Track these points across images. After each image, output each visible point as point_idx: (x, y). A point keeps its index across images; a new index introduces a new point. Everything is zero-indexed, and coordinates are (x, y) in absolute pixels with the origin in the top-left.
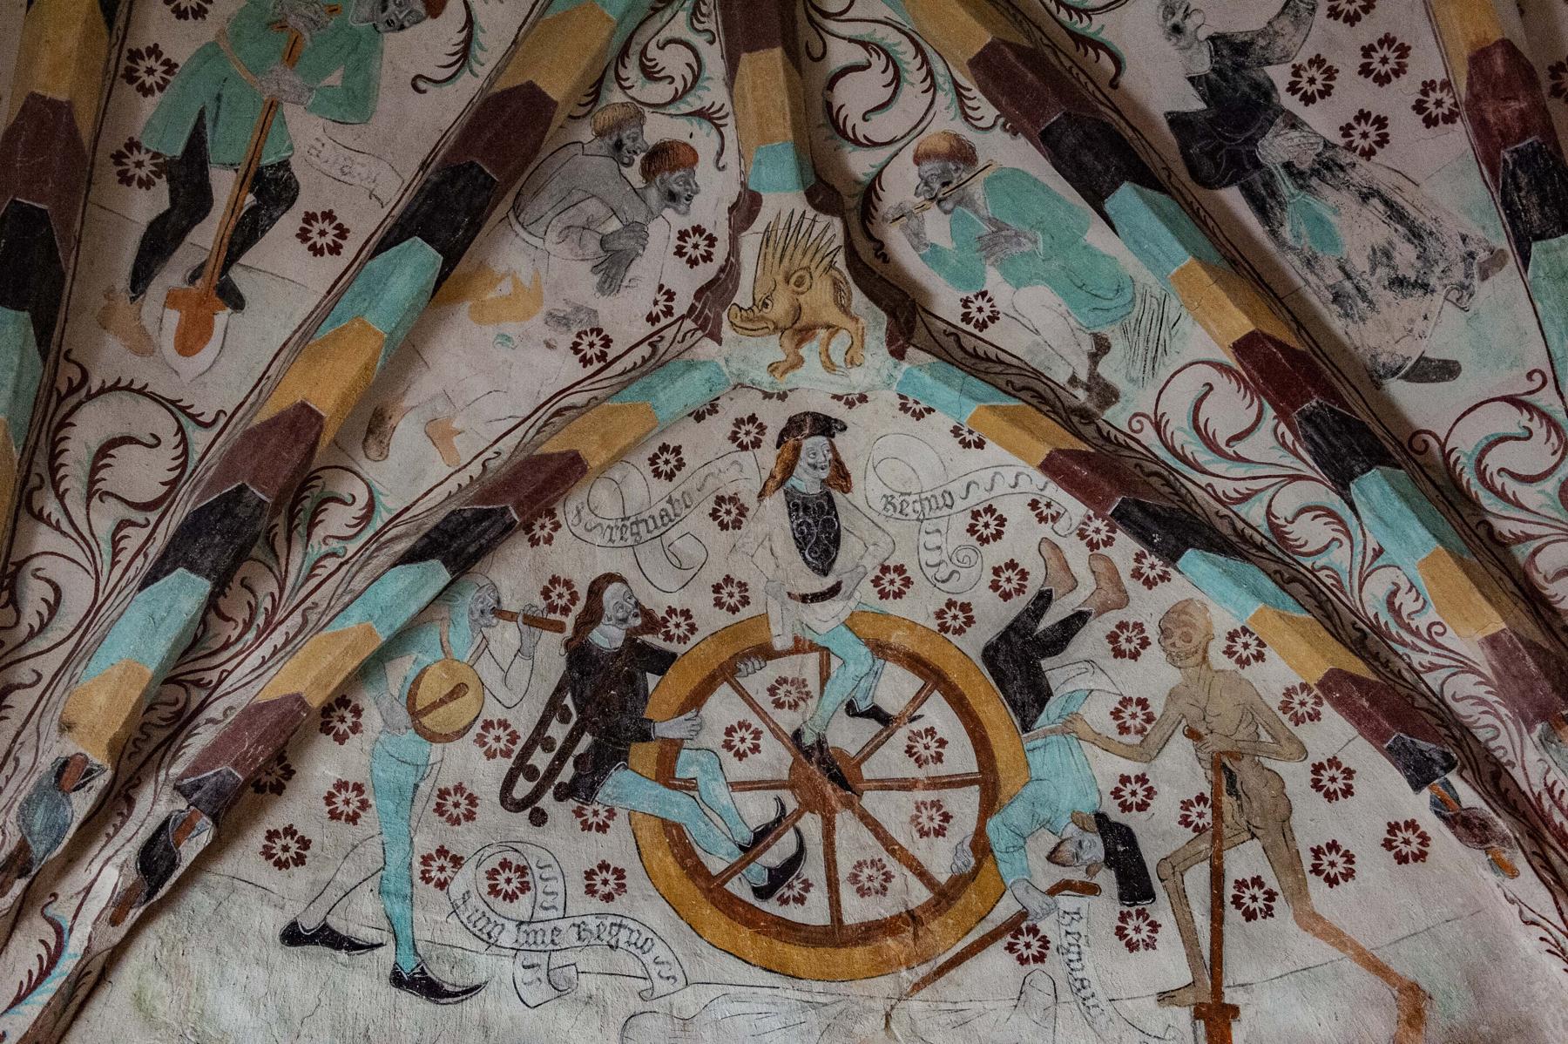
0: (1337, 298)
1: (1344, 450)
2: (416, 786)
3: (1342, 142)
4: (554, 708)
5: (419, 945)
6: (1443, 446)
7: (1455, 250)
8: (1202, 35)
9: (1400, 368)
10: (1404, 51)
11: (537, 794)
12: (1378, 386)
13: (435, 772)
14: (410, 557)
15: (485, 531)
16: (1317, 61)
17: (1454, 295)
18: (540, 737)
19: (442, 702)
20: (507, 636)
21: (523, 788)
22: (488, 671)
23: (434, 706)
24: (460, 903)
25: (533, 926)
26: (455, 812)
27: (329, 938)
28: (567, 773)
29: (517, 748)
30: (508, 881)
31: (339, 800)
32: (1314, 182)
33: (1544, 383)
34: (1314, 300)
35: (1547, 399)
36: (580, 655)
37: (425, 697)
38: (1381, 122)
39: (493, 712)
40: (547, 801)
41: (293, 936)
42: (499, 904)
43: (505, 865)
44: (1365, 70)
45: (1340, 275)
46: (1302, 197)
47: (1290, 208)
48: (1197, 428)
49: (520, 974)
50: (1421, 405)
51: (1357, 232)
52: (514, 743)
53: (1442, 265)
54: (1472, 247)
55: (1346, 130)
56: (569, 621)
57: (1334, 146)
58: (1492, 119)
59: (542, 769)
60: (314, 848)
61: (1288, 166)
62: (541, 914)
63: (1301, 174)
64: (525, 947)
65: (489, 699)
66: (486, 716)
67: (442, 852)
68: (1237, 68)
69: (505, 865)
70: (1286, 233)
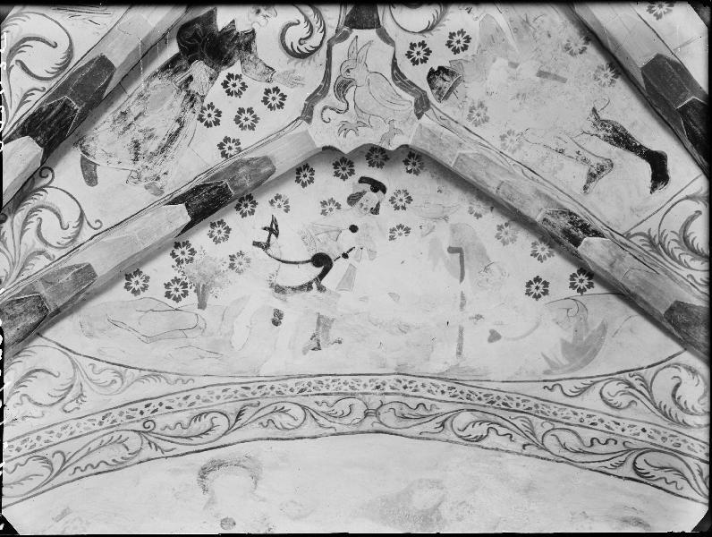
0: (124, 114)
1: (49, 129)
3: (205, 105)
6: (46, 186)
7: (157, 170)
8: (256, 27)
9: (87, 154)
10: (252, 127)
12: (75, 144)
16: (244, 87)
17: (134, 174)
32: (184, 93)
33: (95, 229)
34: (120, 102)
35: (87, 232)
38: (217, 123)
44: (241, 111)
45: (136, 114)
46: (174, 87)
47: (169, 82)
48: (25, 40)
50: (68, 169)
51: (160, 120)
53: (150, 166)
54: (162, 177)
55: (211, 106)
57: (203, 101)
58: (241, 171)
61: (191, 78)
63: (187, 86)
68: (239, 46)
70: (156, 81)
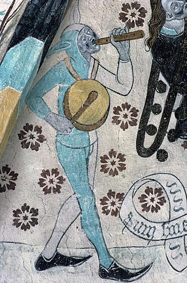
2: (87, 160)
4: (153, 86)
5: (110, 251)
11: (158, 142)
13: (95, 148)
14: (16, 41)
15: (50, 8)
18: (150, 107)
19: (85, 106)
20: (109, 53)
21: (149, 140)
22: (105, 78)
23: (82, 110)
24: (127, 221)
25: (171, 223)
26: (113, 168)
27: (61, 260)
28: (173, 122)
29: (139, 118)
30: (152, 200)
31: (47, 182)
36: (160, 47)
37: (74, 107)
39: (117, 101)
40: (165, 144)
41: (42, 264)
42: (150, 215)
43: (149, 190)
49: (169, 252)
52: (136, 115)
56: (145, 28)
59: (157, 125)
60: (41, 212)
62: (175, 215)
64: (169, 237)
65: (112, 94)
66: (114, 104)
67: (111, 194)
69: (149, 190)
